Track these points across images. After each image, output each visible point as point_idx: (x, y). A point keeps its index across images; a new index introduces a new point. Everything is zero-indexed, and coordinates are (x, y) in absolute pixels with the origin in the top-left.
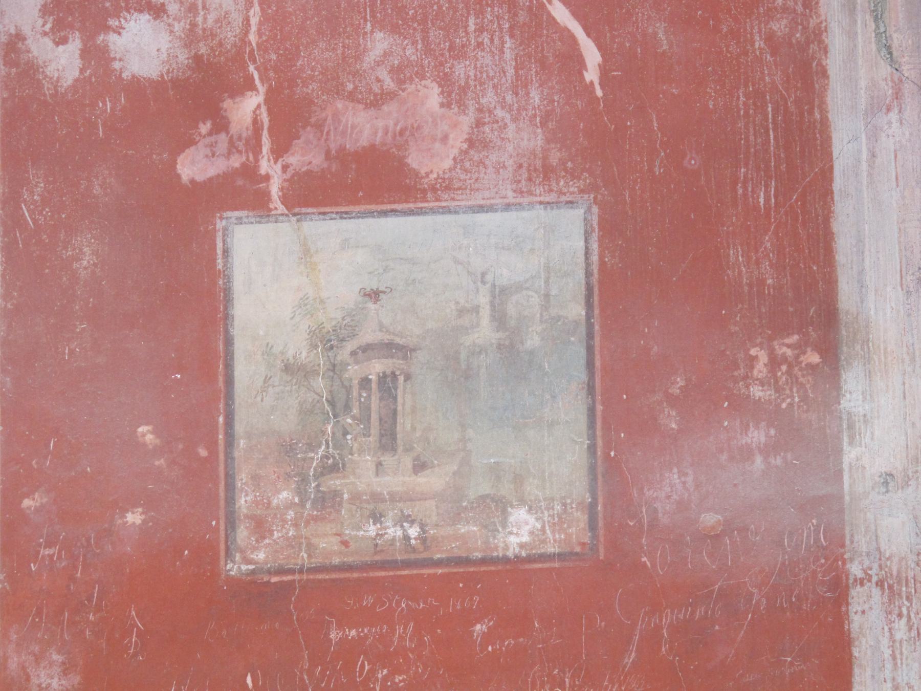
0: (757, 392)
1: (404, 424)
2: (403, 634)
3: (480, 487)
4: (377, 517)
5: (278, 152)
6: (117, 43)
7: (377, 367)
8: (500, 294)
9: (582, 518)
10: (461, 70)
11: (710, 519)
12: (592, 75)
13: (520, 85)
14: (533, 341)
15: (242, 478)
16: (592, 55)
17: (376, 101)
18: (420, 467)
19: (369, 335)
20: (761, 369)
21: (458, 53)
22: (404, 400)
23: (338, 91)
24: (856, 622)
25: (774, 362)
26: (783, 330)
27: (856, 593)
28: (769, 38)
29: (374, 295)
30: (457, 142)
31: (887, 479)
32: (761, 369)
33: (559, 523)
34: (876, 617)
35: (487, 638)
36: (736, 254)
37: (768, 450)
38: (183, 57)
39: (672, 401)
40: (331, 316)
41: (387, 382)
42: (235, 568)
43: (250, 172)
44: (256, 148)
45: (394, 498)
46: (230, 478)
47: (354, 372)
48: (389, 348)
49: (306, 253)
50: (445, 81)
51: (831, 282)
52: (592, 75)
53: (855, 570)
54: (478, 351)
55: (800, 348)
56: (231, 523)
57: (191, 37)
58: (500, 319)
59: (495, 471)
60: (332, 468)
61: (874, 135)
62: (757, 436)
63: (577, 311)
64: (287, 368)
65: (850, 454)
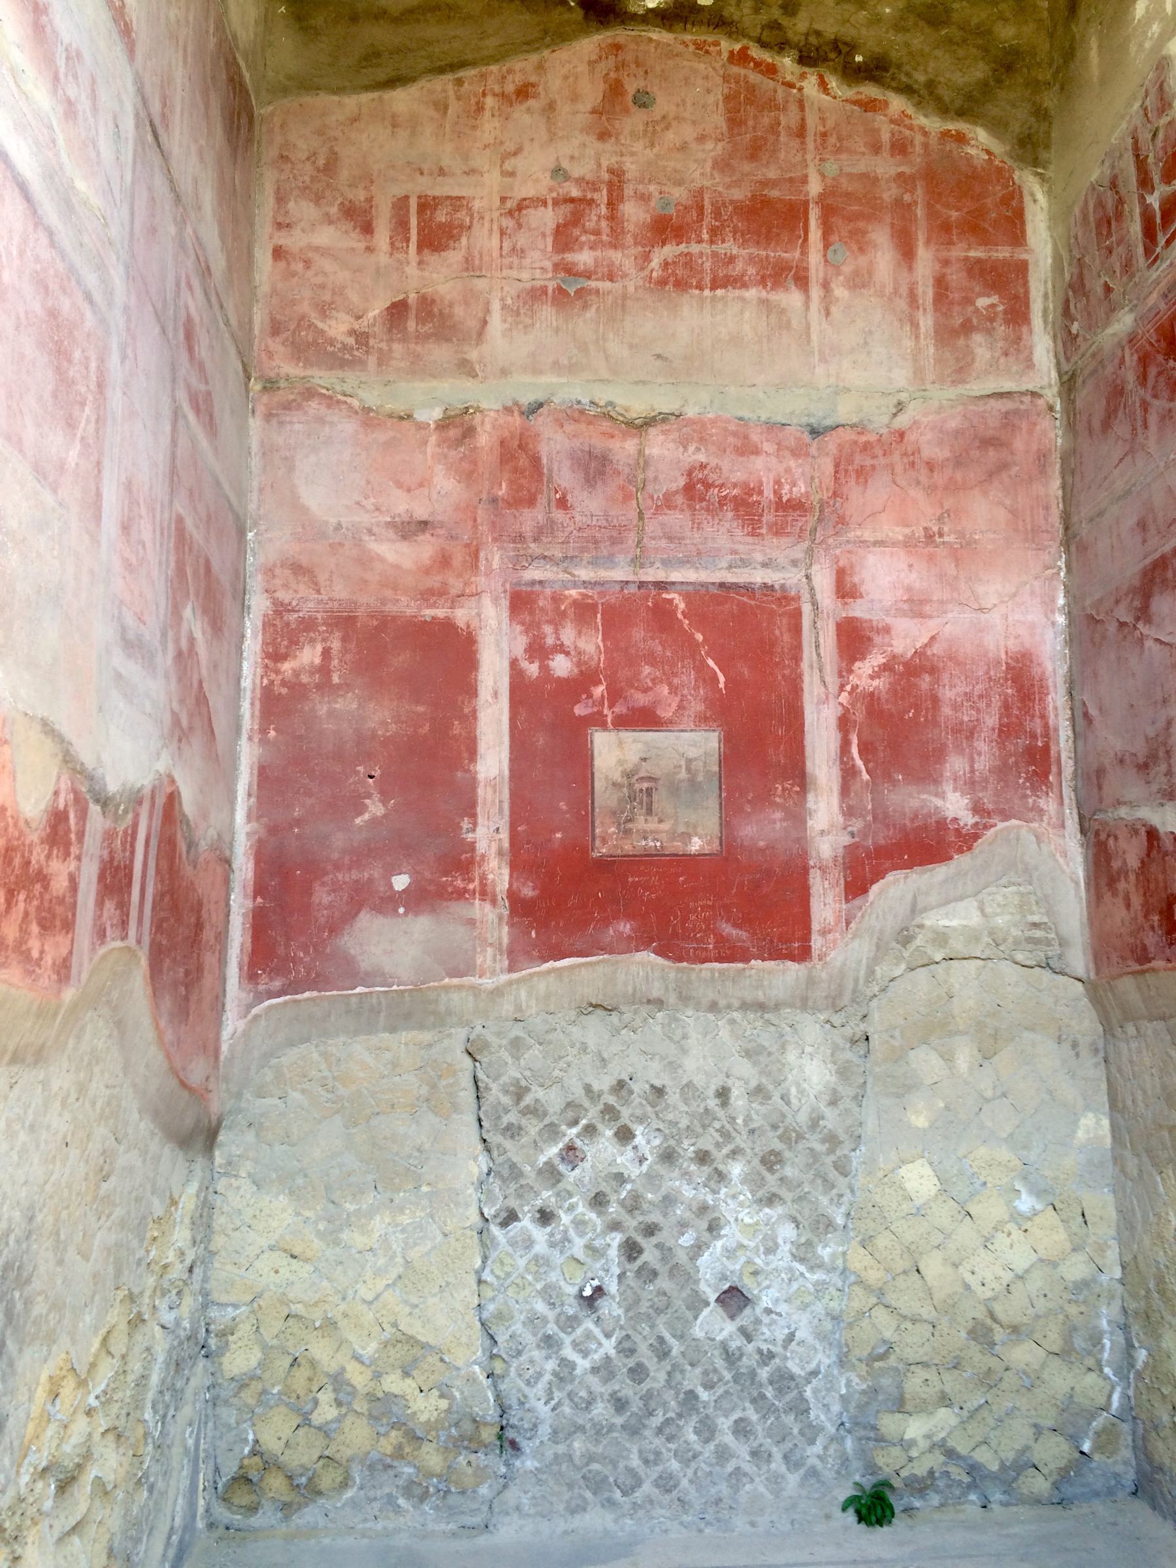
0: (778, 800)
1: (655, 806)
2: (655, 880)
3: (682, 829)
4: (645, 839)
5: (610, 707)
6: (551, 664)
7: (645, 785)
8: (689, 761)
9: (717, 842)
10: (676, 681)
11: (762, 844)
12: (722, 685)
13: (696, 688)
14: (700, 778)
15: (597, 823)
16: (722, 678)
17: (646, 690)
18: (661, 821)
19: (642, 774)
20: (779, 791)
21: (675, 675)
22: (655, 797)
23: (632, 686)
24: (811, 881)
25: (784, 790)
26: (786, 779)
27: (812, 871)
28: (783, 676)
29: (644, 760)
30: (674, 706)
31: (822, 832)
32: (779, 791)
33: (709, 843)
34: (818, 879)
35: (684, 882)
36: (771, 751)
37: (781, 820)
38: (576, 671)
39: (749, 802)
40: (629, 766)
41: (649, 792)
42: (595, 854)
43: (600, 713)
44: (602, 704)
45: (652, 832)
46: (593, 822)
47: (637, 786)
48: (650, 779)
49: (620, 744)
50: (670, 684)
51: (804, 763)
52: (722, 685)
53: (811, 863)
54: (682, 781)
55: (793, 785)
56: (593, 840)
57: (579, 664)
58: (689, 770)
59: (687, 824)
60: (630, 820)
61: (819, 712)
62: (778, 815)
63: (716, 768)
64: (614, 784)
65: (810, 823)
